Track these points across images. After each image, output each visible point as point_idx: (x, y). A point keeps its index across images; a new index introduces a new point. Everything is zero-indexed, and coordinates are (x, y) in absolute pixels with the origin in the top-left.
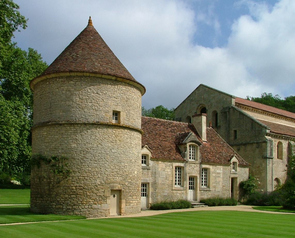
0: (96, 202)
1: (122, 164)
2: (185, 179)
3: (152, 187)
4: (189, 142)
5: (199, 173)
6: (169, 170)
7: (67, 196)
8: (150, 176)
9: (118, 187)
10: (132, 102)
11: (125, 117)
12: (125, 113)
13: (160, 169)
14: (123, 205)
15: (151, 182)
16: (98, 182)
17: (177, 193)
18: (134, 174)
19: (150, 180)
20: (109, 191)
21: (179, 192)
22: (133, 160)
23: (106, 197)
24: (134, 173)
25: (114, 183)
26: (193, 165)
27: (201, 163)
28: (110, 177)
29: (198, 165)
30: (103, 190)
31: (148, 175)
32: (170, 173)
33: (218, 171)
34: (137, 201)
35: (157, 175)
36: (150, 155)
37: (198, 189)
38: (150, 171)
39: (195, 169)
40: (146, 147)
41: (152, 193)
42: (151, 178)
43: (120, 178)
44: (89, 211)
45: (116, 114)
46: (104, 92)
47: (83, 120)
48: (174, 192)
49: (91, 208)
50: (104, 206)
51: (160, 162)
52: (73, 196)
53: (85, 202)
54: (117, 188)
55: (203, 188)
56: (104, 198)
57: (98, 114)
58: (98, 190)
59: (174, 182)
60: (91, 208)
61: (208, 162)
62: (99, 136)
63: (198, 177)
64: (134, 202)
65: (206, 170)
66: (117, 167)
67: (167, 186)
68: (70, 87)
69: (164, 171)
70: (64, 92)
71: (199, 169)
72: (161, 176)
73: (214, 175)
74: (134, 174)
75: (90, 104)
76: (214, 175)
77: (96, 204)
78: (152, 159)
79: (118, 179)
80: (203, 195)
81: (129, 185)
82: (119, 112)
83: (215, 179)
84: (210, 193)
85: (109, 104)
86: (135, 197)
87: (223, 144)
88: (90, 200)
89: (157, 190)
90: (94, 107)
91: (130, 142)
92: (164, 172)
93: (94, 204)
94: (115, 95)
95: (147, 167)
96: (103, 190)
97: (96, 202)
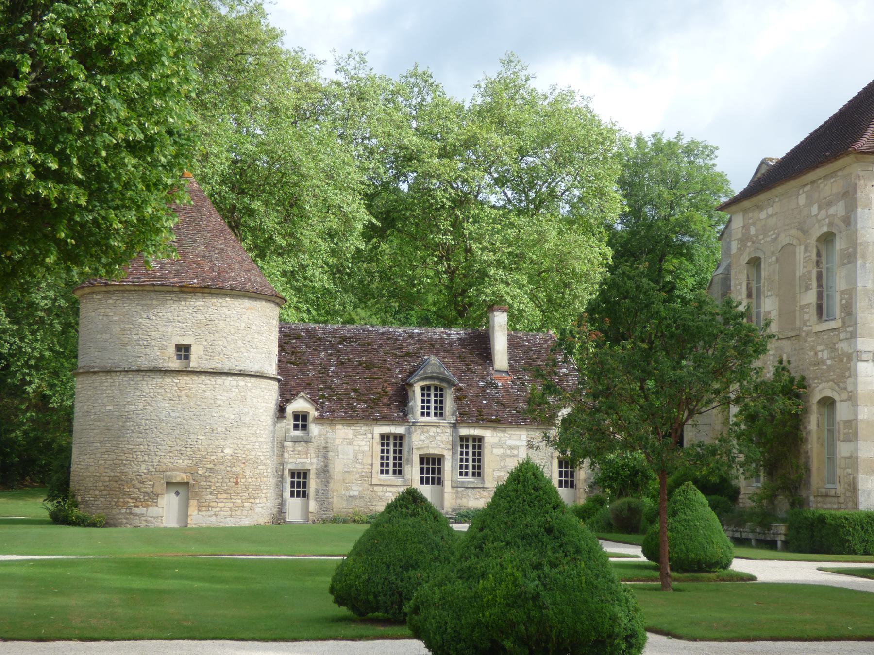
0: (138, 504)
1: (192, 436)
2: (409, 461)
3: (317, 478)
4: (419, 380)
5: (450, 447)
6: (363, 443)
7: (97, 492)
8: (313, 455)
9: (181, 477)
10: (222, 324)
11: (202, 352)
12: (201, 348)
13: (338, 442)
14: (193, 511)
15: (314, 466)
16: (143, 469)
17: (386, 492)
18: (222, 454)
19: (311, 463)
20: (162, 484)
21: (389, 489)
22: (219, 429)
23: (157, 495)
24: (223, 452)
25: (171, 470)
26: (433, 430)
27: (454, 426)
28: (165, 461)
29: (449, 430)
30: (151, 483)
31: (307, 453)
32: (367, 449)
33: (510, 442)
34: (231, 505)
35: (331, 454)
36: (313, 413)
37: (447, 484)
38: (314, 445)
39: (438, 438)
40: (302, 397)
41: (317, 491)
42: (315, 460)
43: (186, 462)
44: (126, 519)
45: (183, 351)
46: (160, 314)
47: (145, 364)
48: (376, 488)
49: (131, 513)
50: (153, 511)
51: (339, 427)
52: (105, 492)
53: (121, 504)
54: (178, 480)
55: (463, 482)
56: (153, 497)
57: (148, 352)
58: (143, 483)
59: (377, 467)
60: (131, 513)
61: (482, 418)
62: (147, 391)
63: (448, 455)
64: (220, 505)
65: (479, 440)
66: (180, 443)
67: (358, 476)
68: (108, 310)
69: (350, 443)
70: (101, 318)
71: (451, 438)
72: (341, 456)
73: (499, 451)
74: (222, 454)
75: (136, 337)
76: (499, 451)
77: (138, 507)
78: (320, 420)
79: (183, 463)
80: (462, 498)
81: (207, 474)
82: (190, 346)
83: (503, 460)
84: (485, 494)
85: (169, 334)
86: (225, 496)
87: (565, 374)
88: (129, 500)
89: (331, 485)
90: (141, 342)
91: (211, 397)
92: (350, 447)
93: (135, 506)
94: (179, 318)
95: (305, 438)
96: (151, 483)
97: (138, 504)
